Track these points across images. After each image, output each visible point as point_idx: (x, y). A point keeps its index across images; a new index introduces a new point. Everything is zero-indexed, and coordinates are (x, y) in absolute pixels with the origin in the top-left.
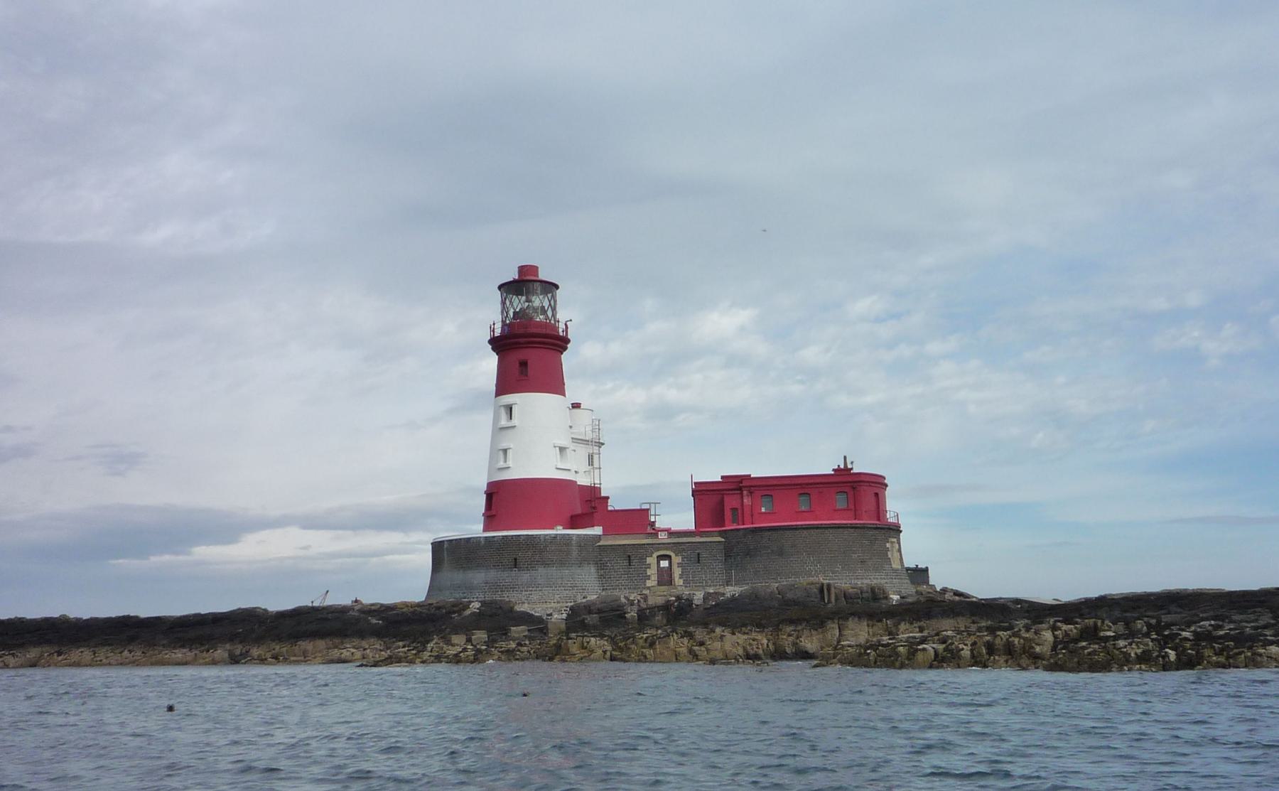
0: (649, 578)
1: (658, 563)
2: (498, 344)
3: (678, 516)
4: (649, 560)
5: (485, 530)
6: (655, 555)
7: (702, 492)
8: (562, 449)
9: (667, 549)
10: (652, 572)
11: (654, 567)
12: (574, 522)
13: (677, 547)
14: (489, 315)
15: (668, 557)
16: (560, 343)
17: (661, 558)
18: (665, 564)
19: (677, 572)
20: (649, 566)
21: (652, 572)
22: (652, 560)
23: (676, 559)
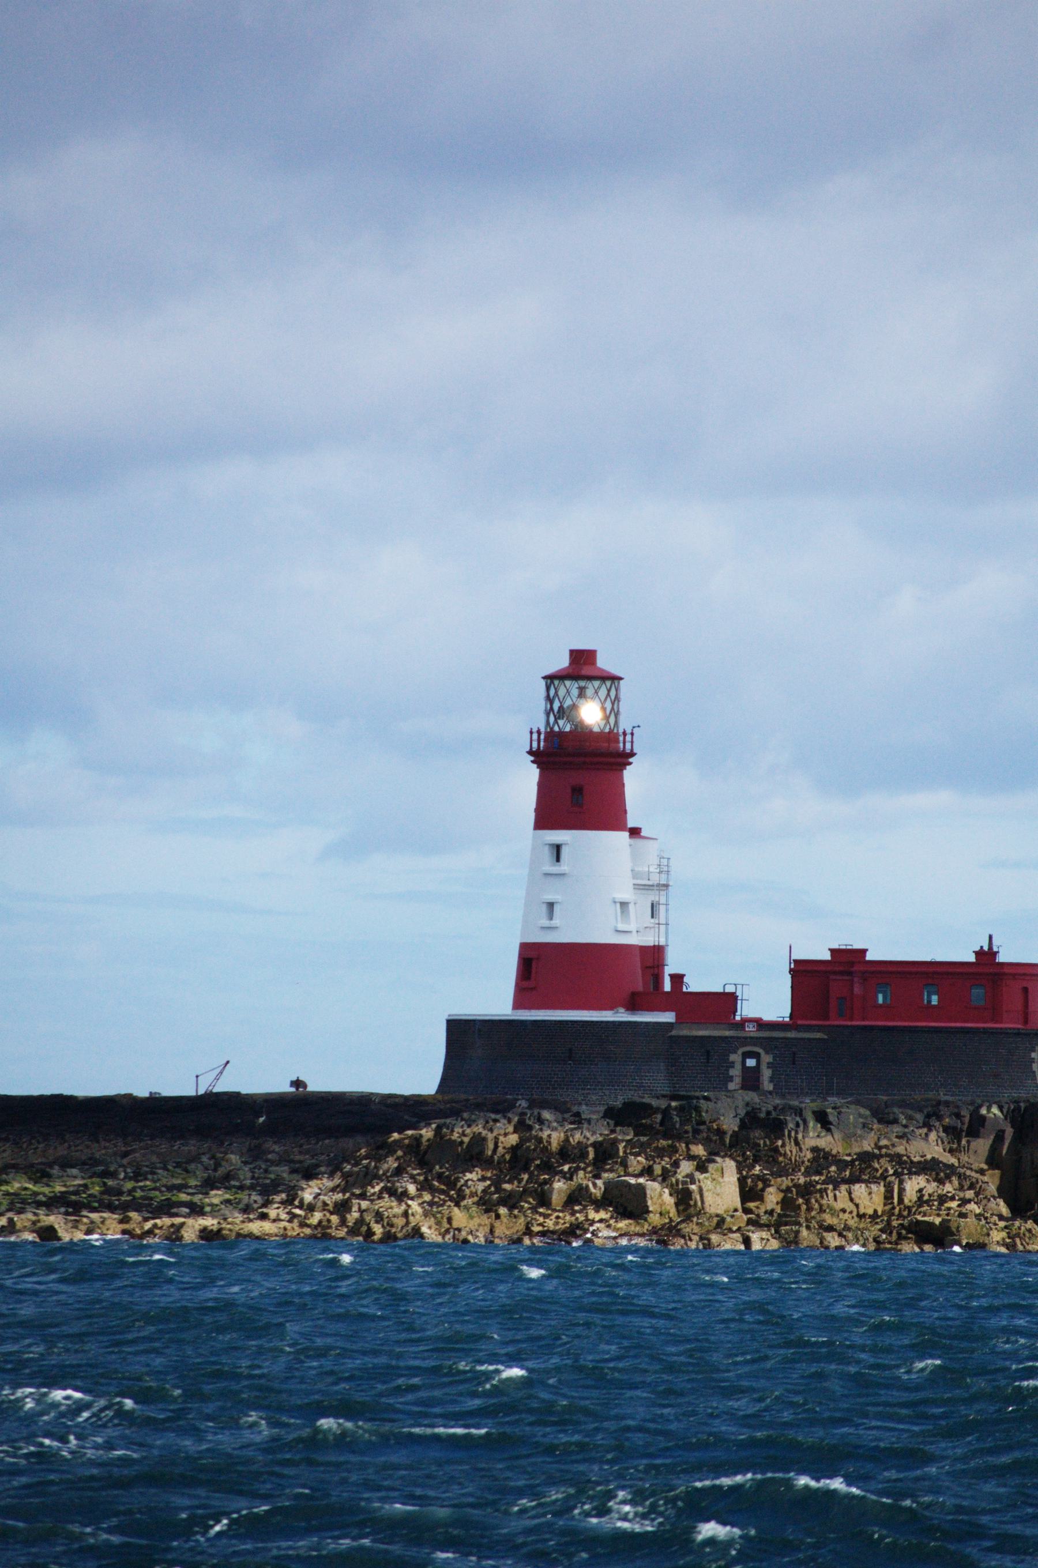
0: (731, 1079)
1: (744, 1063)
2: (538, 757)
3: (768, 1000)
4: (733, 1057)
5: (518, 1005)
6: (740, 1051)
7: (804, 973)
8: (624, 905)
9: (755, 1045)
10: (736, 1072)
11: (738, 1066)
12: (633, 1005)
13: (768, 1044)
14: (529, 717)
15: (756, 1055)
16: (622, 759)
17: (747, 1055)
18: (751, 1063)
19: (766, 1073)
20: (732, 1065)
21: (736, 1072)
22: (735, 1058)
23: (766, 1058)
